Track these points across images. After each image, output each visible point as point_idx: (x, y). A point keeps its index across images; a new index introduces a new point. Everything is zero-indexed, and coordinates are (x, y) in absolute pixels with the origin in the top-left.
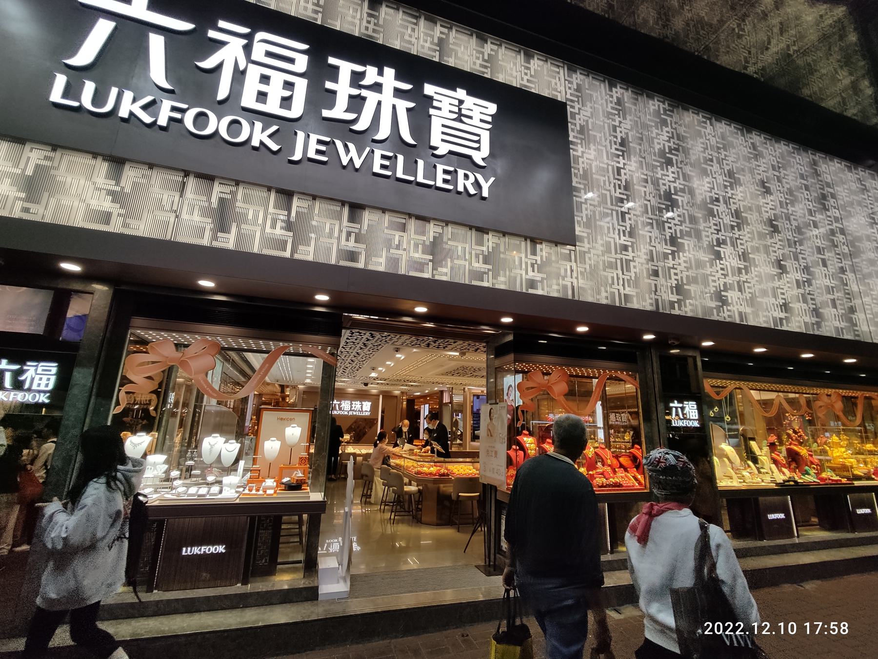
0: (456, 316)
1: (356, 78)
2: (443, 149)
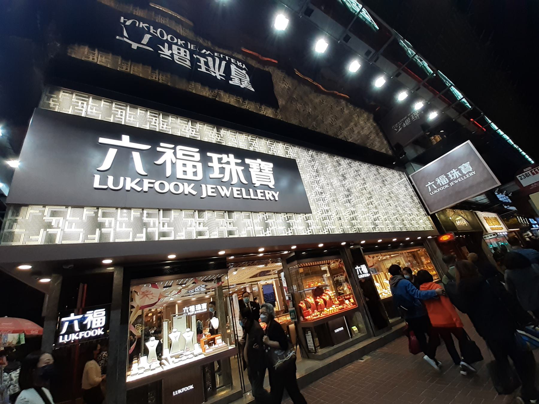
0: (275, 249)
1: (220, 160)
2: (258, 184)
